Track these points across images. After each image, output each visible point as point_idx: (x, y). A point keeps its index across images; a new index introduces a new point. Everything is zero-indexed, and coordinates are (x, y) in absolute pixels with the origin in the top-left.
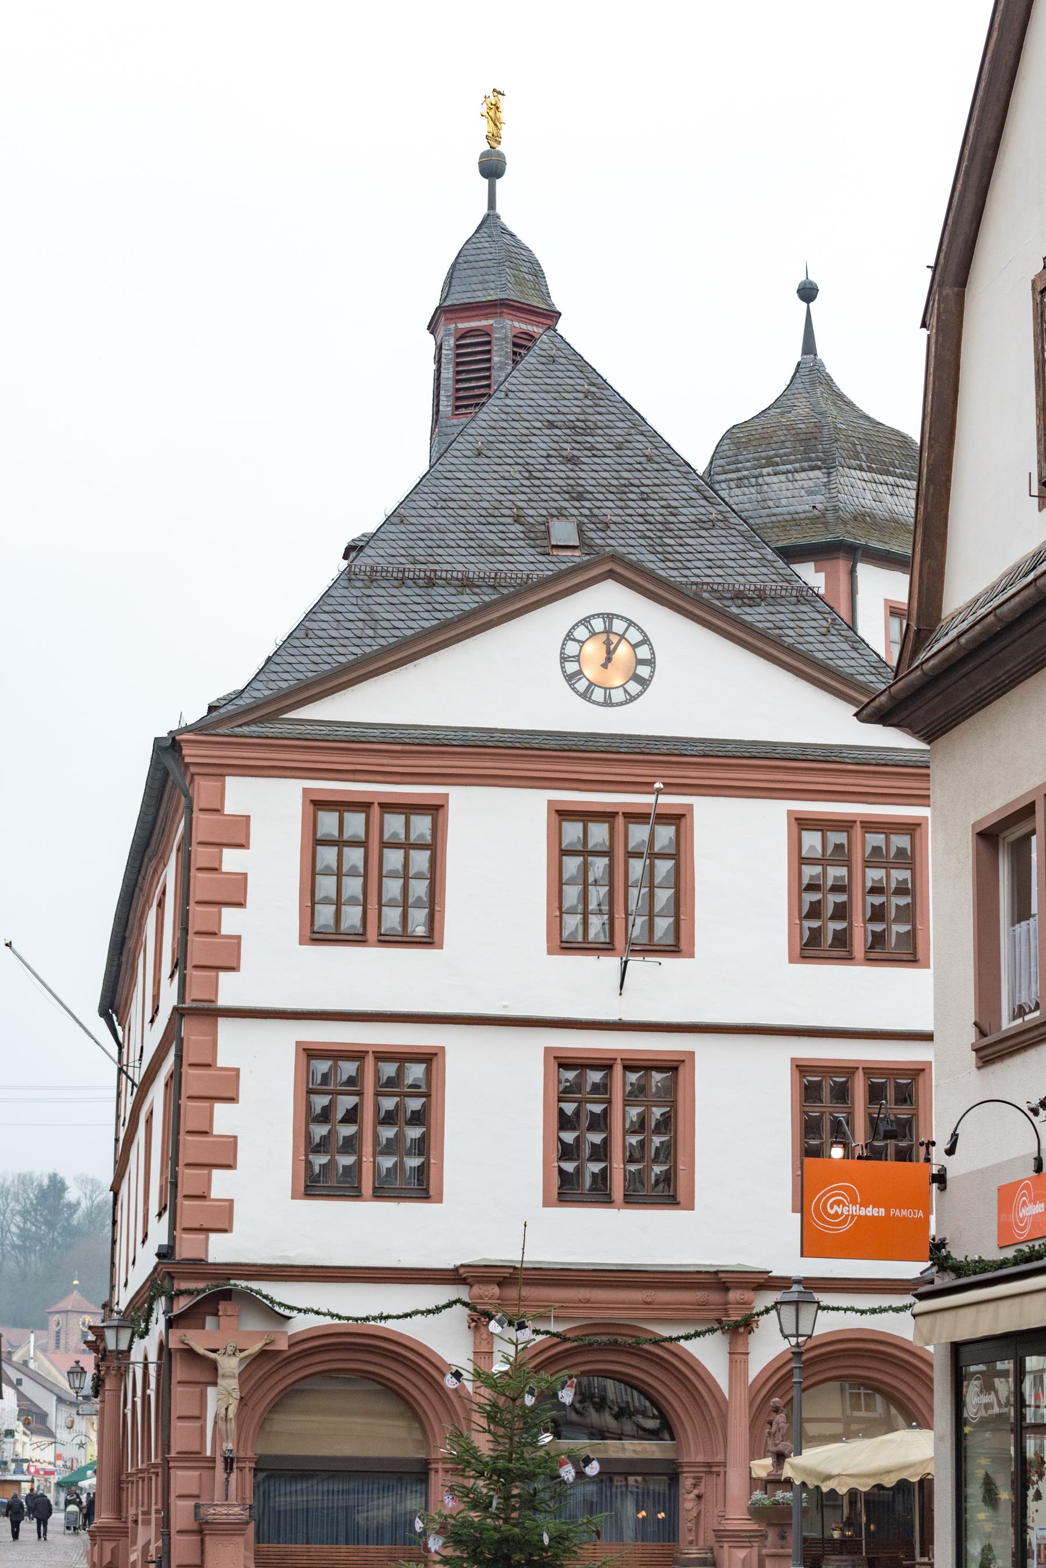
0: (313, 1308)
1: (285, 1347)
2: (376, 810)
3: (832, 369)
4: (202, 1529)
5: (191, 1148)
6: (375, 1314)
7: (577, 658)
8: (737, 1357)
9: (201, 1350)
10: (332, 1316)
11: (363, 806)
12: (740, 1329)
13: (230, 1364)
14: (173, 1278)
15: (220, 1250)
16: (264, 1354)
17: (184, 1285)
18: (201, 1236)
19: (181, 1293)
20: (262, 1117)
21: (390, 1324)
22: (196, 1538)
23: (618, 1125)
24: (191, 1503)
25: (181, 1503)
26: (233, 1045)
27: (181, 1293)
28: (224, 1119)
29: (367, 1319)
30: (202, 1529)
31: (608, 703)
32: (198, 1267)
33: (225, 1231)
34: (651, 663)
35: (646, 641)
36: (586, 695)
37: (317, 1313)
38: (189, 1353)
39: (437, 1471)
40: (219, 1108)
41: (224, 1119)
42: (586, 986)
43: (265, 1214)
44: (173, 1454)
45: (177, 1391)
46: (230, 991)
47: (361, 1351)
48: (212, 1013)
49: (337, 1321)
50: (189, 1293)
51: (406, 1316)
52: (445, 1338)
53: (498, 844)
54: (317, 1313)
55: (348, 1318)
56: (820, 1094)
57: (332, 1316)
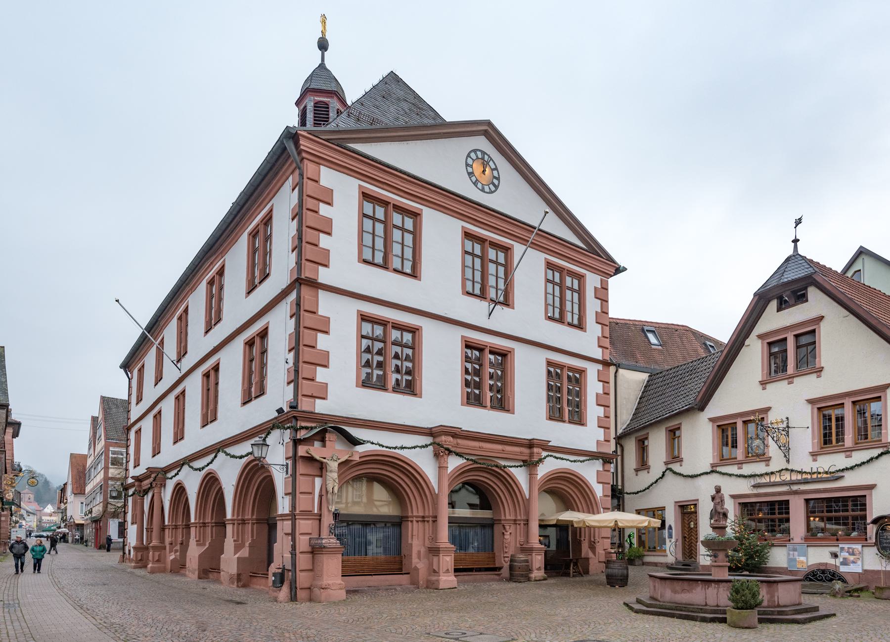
0: (374, 441)
1: (357, 459)
2: (391, 207)
3: (328, 67)
4: (315, 550)
5: (306, 354)
6: (399, 446)
7: (471, 166)
8: (532, 476)
9: (318, 458)
10: (380, 445)
11: (384, 203)
12: (530, 464)
13: (334, 465)
14: (297, 420)
15: (321, 407)
16: (347, 462)
17: (304, 424)
18: (312, 400)
19: (302, 428)
20: (341, 343)
21: (397, 451)
22: (310, 556)
23: (486, 374)
24: (308, 537)
25: (302, 537)
26: (327, 304)
27: (302, 428)
28: (323, 342)
29: (395, 448)
30: (315, 550)
31: (483, 190)
32: (311, 416)
33: (324, 399)
34: (498, 179)
35: (496, 169)
36: (475, 184)
37: (372, 443)
38: (310, 459)
39: (412, 521)
40: (320, 336)
41: (323, 342)
42: (474, 311)
43: (342, 392)
44: (297, 512)
45: (300, 479)
46: (324, 276)
47: (383, 464)
48: (315, 285)
49: (381, 448)
50: (306, 428)
51: (412, 448)
52: (424, 461)
53: (442, 238)
54: (372, 443)
55: (387, 447)
56: (554, 372)
57: (380, 445)
